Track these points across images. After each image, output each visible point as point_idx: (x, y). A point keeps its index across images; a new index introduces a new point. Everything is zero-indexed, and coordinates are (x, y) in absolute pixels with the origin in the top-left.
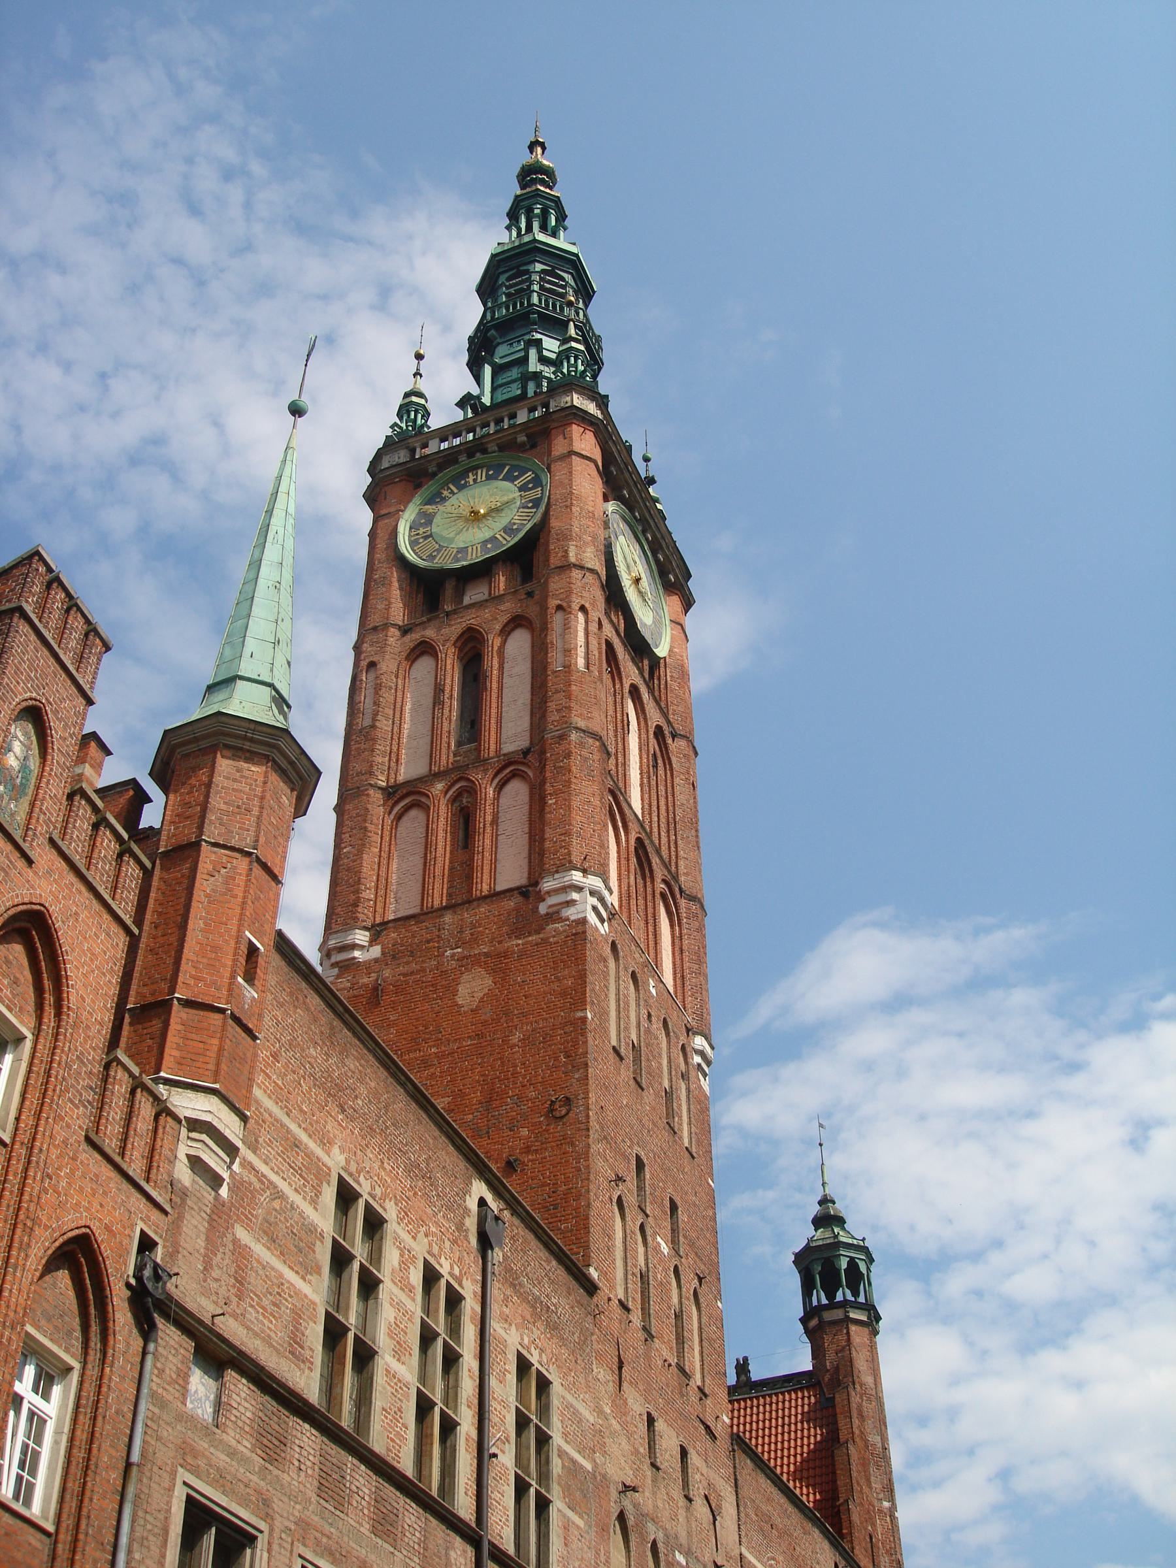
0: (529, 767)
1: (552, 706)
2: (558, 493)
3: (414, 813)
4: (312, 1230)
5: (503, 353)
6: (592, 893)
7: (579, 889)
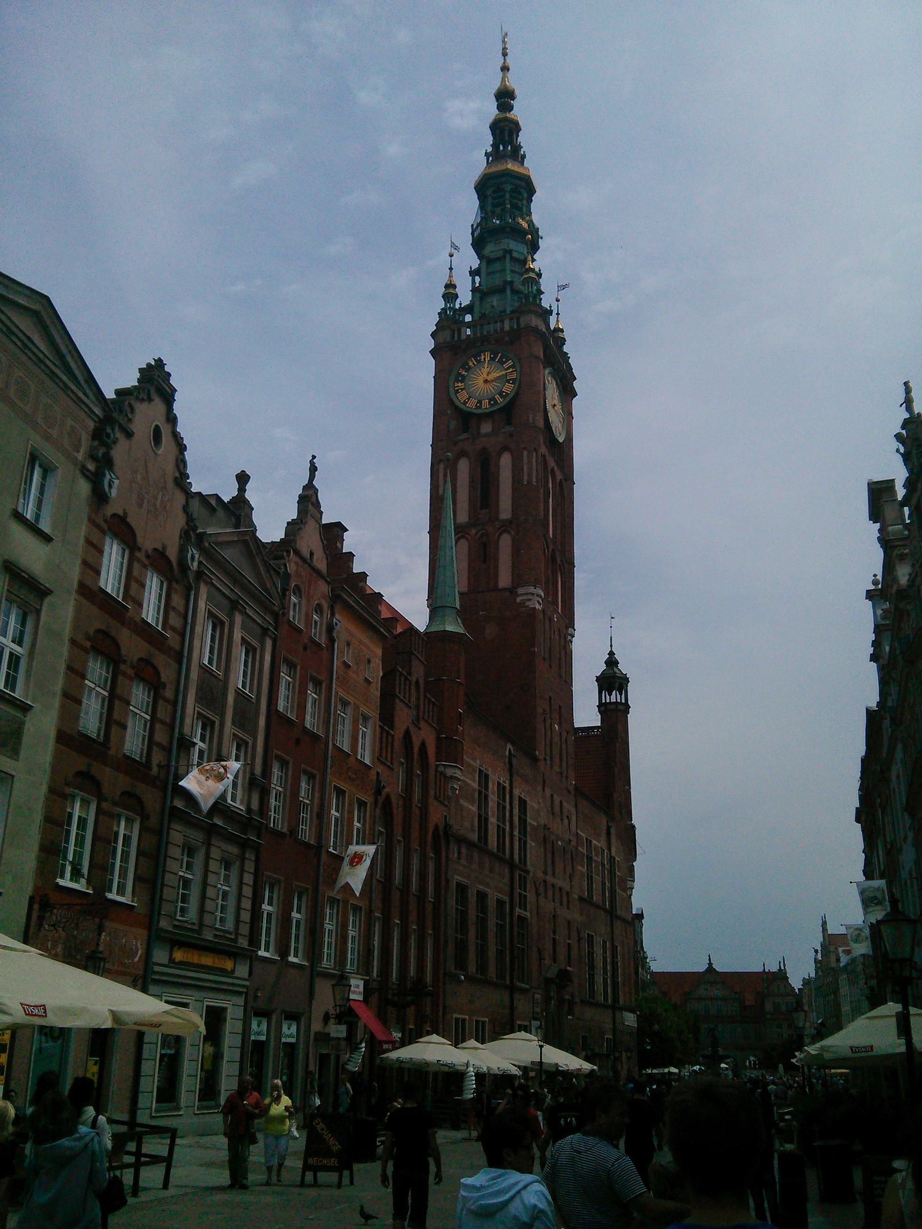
3: (462, 541)
4: (474, 790)
5: (490, 249)
6: (538, 595)
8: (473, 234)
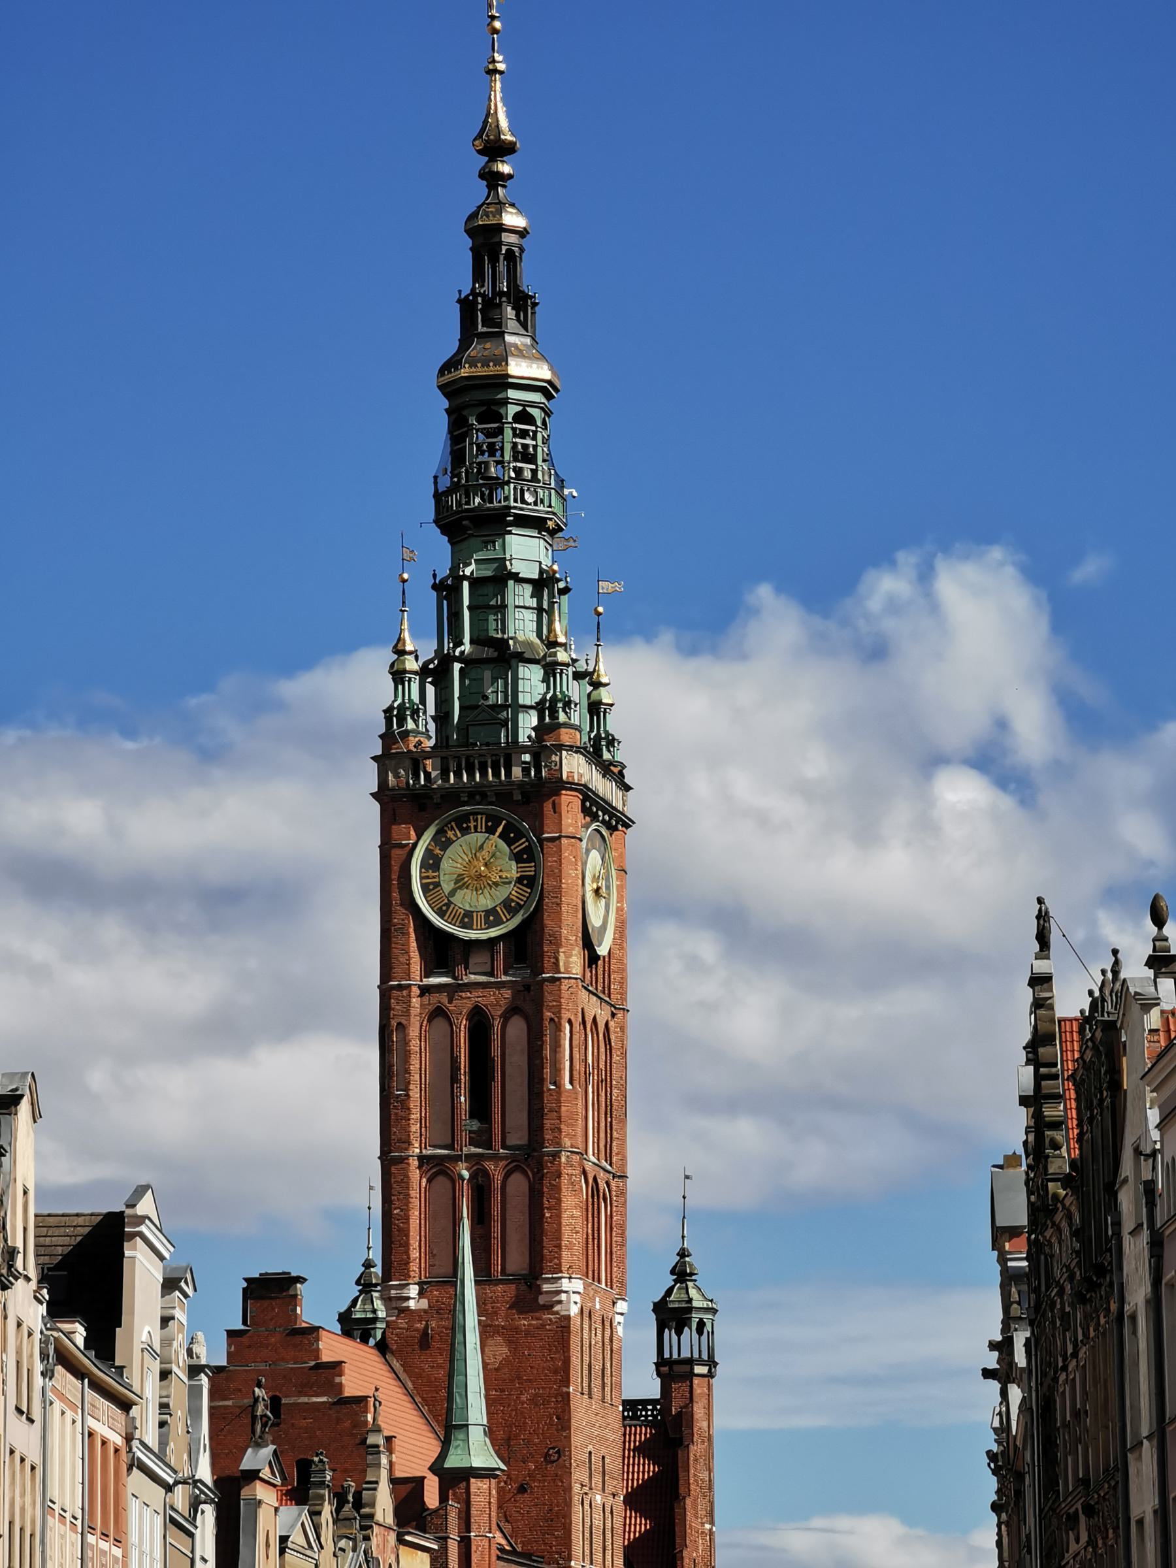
0: (528, 1166)
1: (548, 1123)
2: (550, 883)
3: (441, 1178)
7: (566, 1292)
8: (437, 496)
